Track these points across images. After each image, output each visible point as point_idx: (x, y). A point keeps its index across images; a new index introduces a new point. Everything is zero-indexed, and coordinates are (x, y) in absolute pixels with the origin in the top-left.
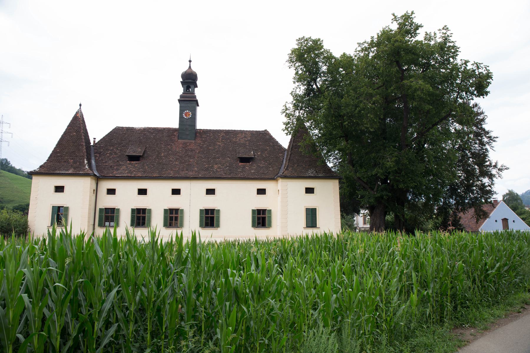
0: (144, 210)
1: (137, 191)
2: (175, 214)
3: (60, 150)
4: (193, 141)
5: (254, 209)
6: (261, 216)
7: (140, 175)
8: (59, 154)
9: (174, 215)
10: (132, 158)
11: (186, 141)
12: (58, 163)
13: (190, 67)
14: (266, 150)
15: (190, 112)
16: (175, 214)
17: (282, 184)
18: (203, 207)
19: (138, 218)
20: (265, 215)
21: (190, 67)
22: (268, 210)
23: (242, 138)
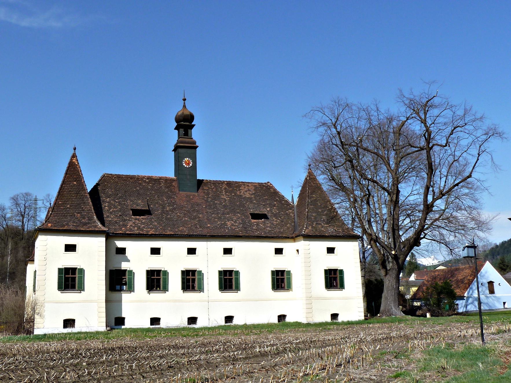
0: (73, 270)
1: (186, 251)
2: (192, 276)
3: (63, 202)
4: (196, 194)
5: (61, 267)
6: (228, 277)
7: (71, 228)
8: (62, 208)
9: (191, 277)
10: (137, 212)
11: (189, 193)
12: (64, 218)
13: (184, 106)
14: (274, 205)
15: (185, 160)
16: (192, 276)
17: (302, 244)
18: (274, 268)
19: (67, 279)
20: (75, 274)
21: (184, 106)
22: (79, 269)
23: (246, 191)
